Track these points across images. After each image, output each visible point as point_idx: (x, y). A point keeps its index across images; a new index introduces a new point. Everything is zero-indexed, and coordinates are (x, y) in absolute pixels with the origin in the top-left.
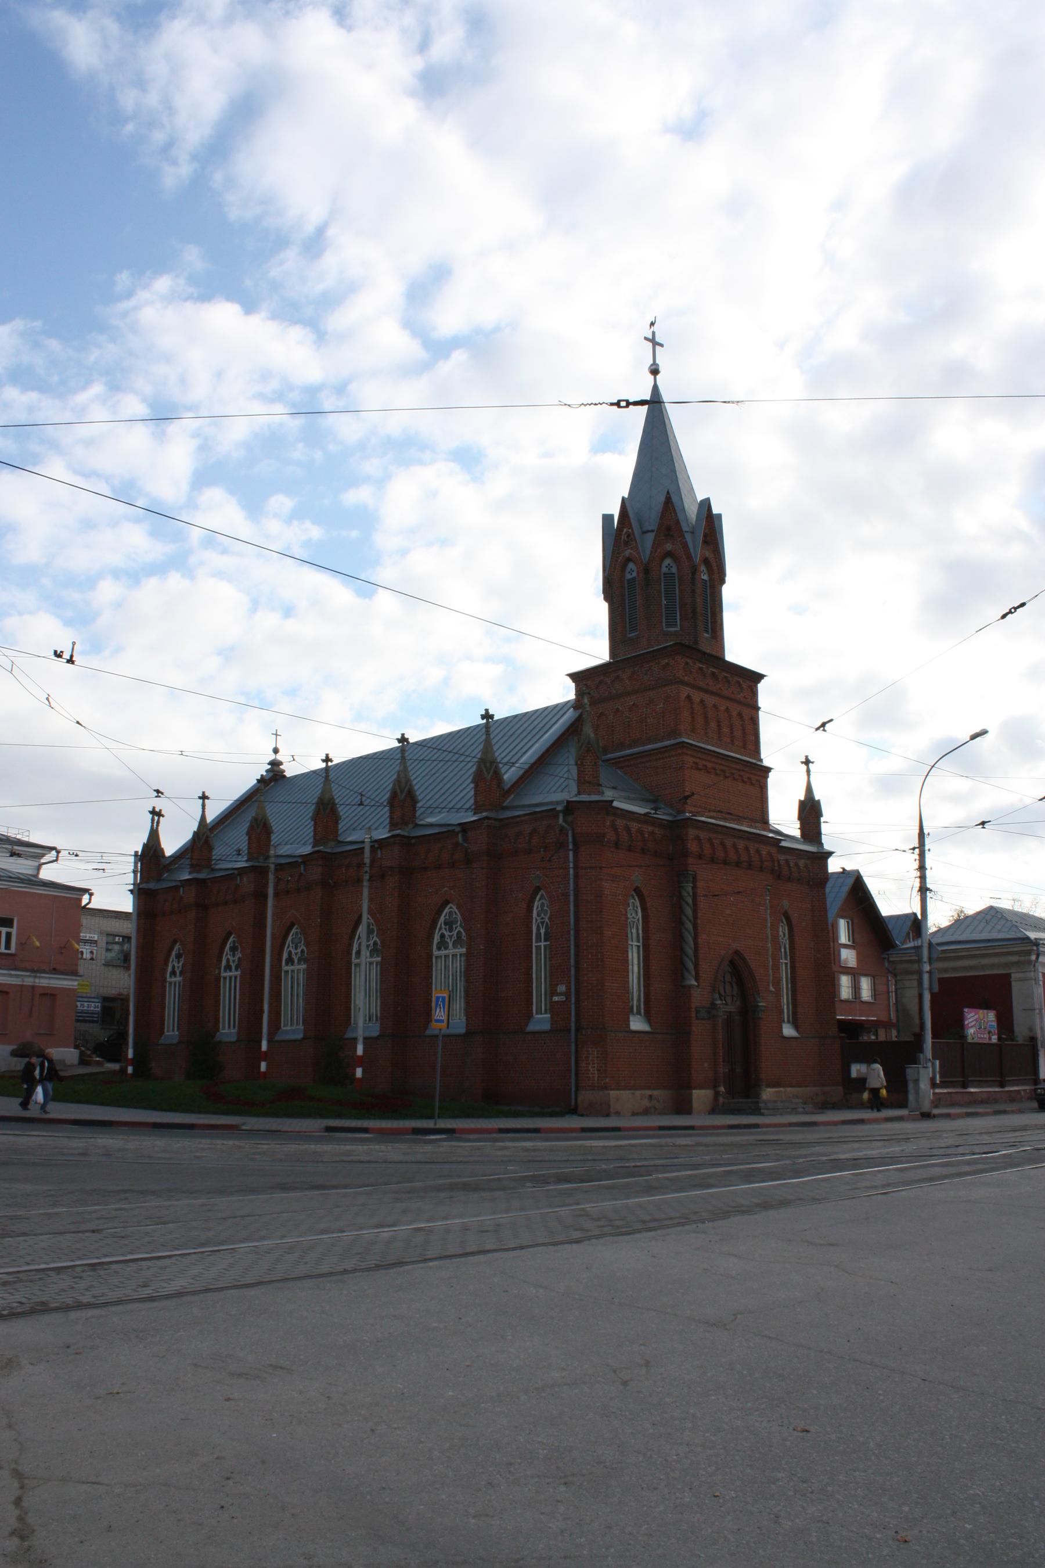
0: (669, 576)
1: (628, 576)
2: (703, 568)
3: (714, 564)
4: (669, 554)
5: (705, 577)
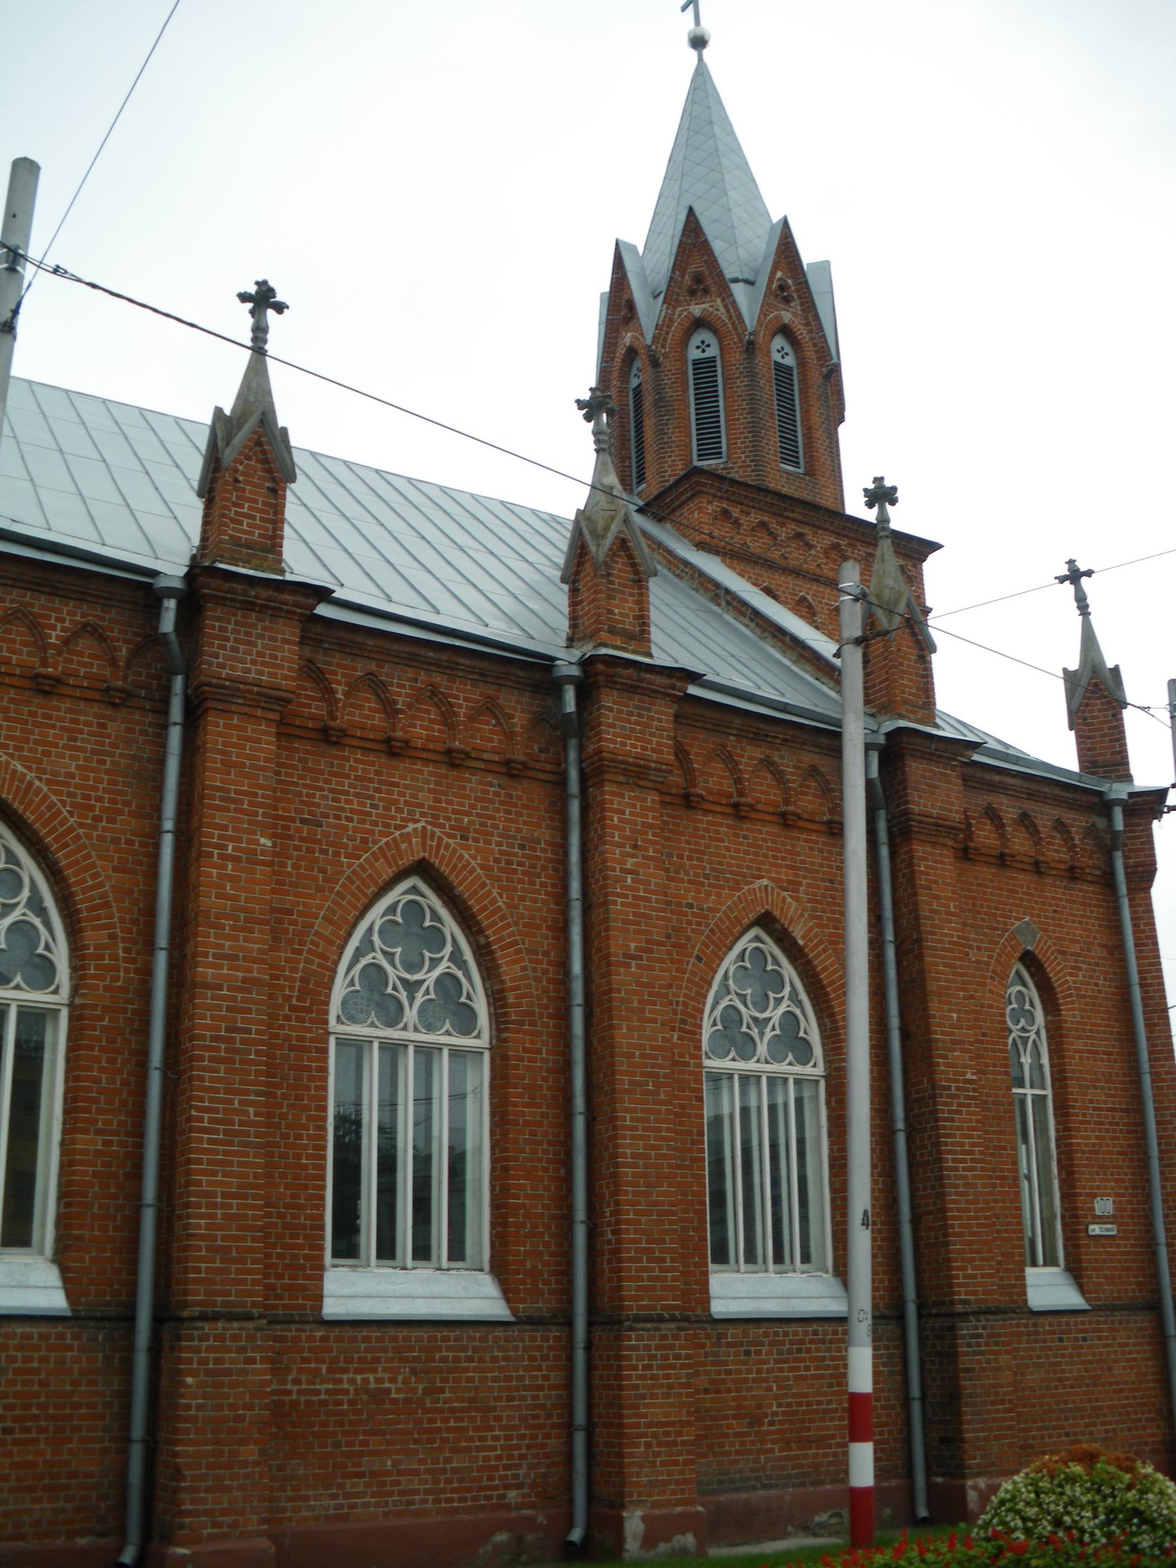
0: (705, 367)
2: (779, 342)
3: (802, 333)
4: (699, 323)
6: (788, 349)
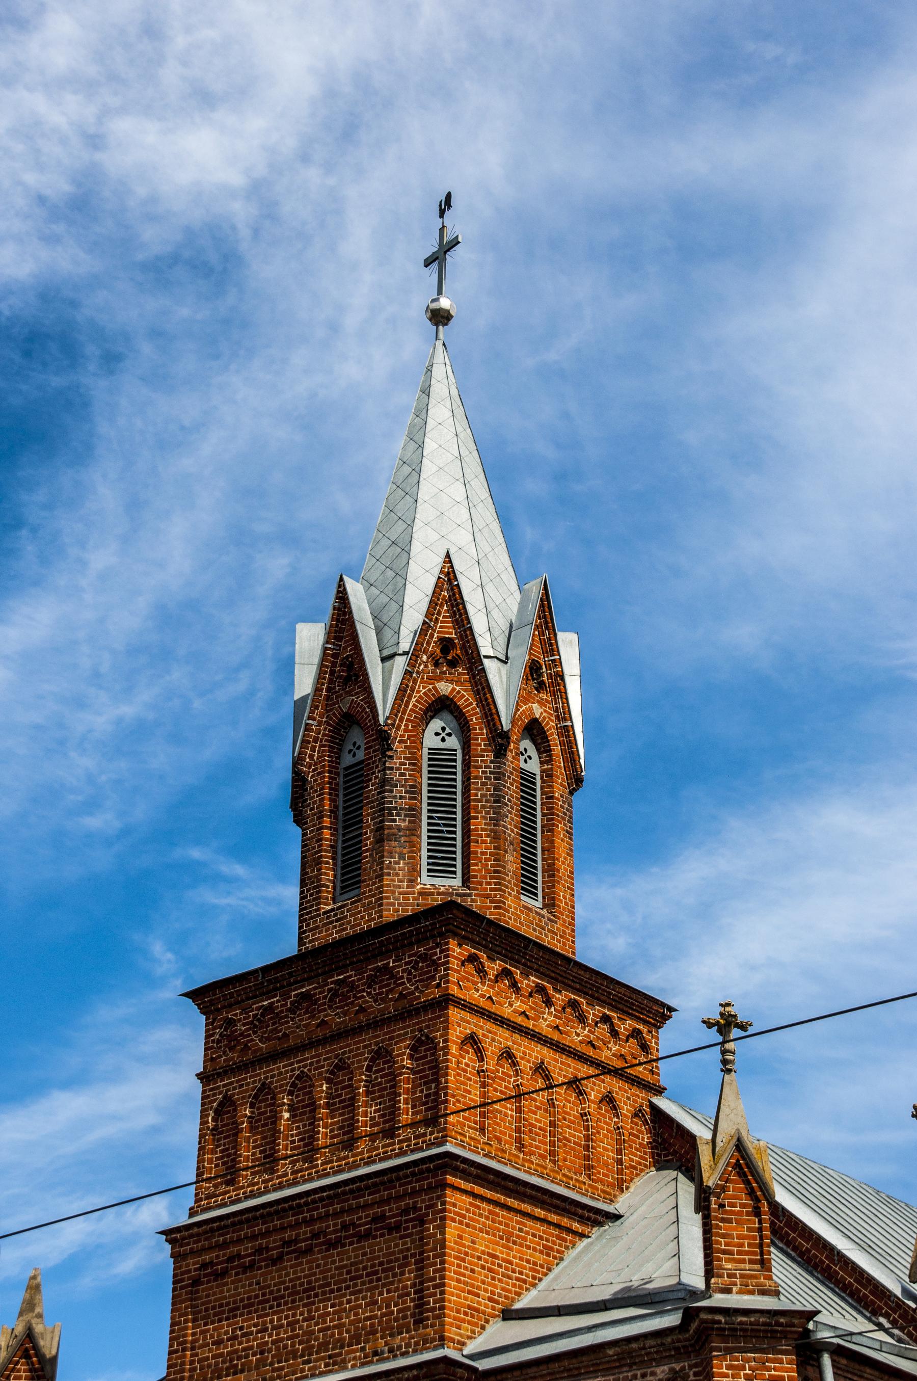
1: (348, 760)
3: (554, 739)
4: (441, 706)
5: (534, 766)
6: (532, 751)
